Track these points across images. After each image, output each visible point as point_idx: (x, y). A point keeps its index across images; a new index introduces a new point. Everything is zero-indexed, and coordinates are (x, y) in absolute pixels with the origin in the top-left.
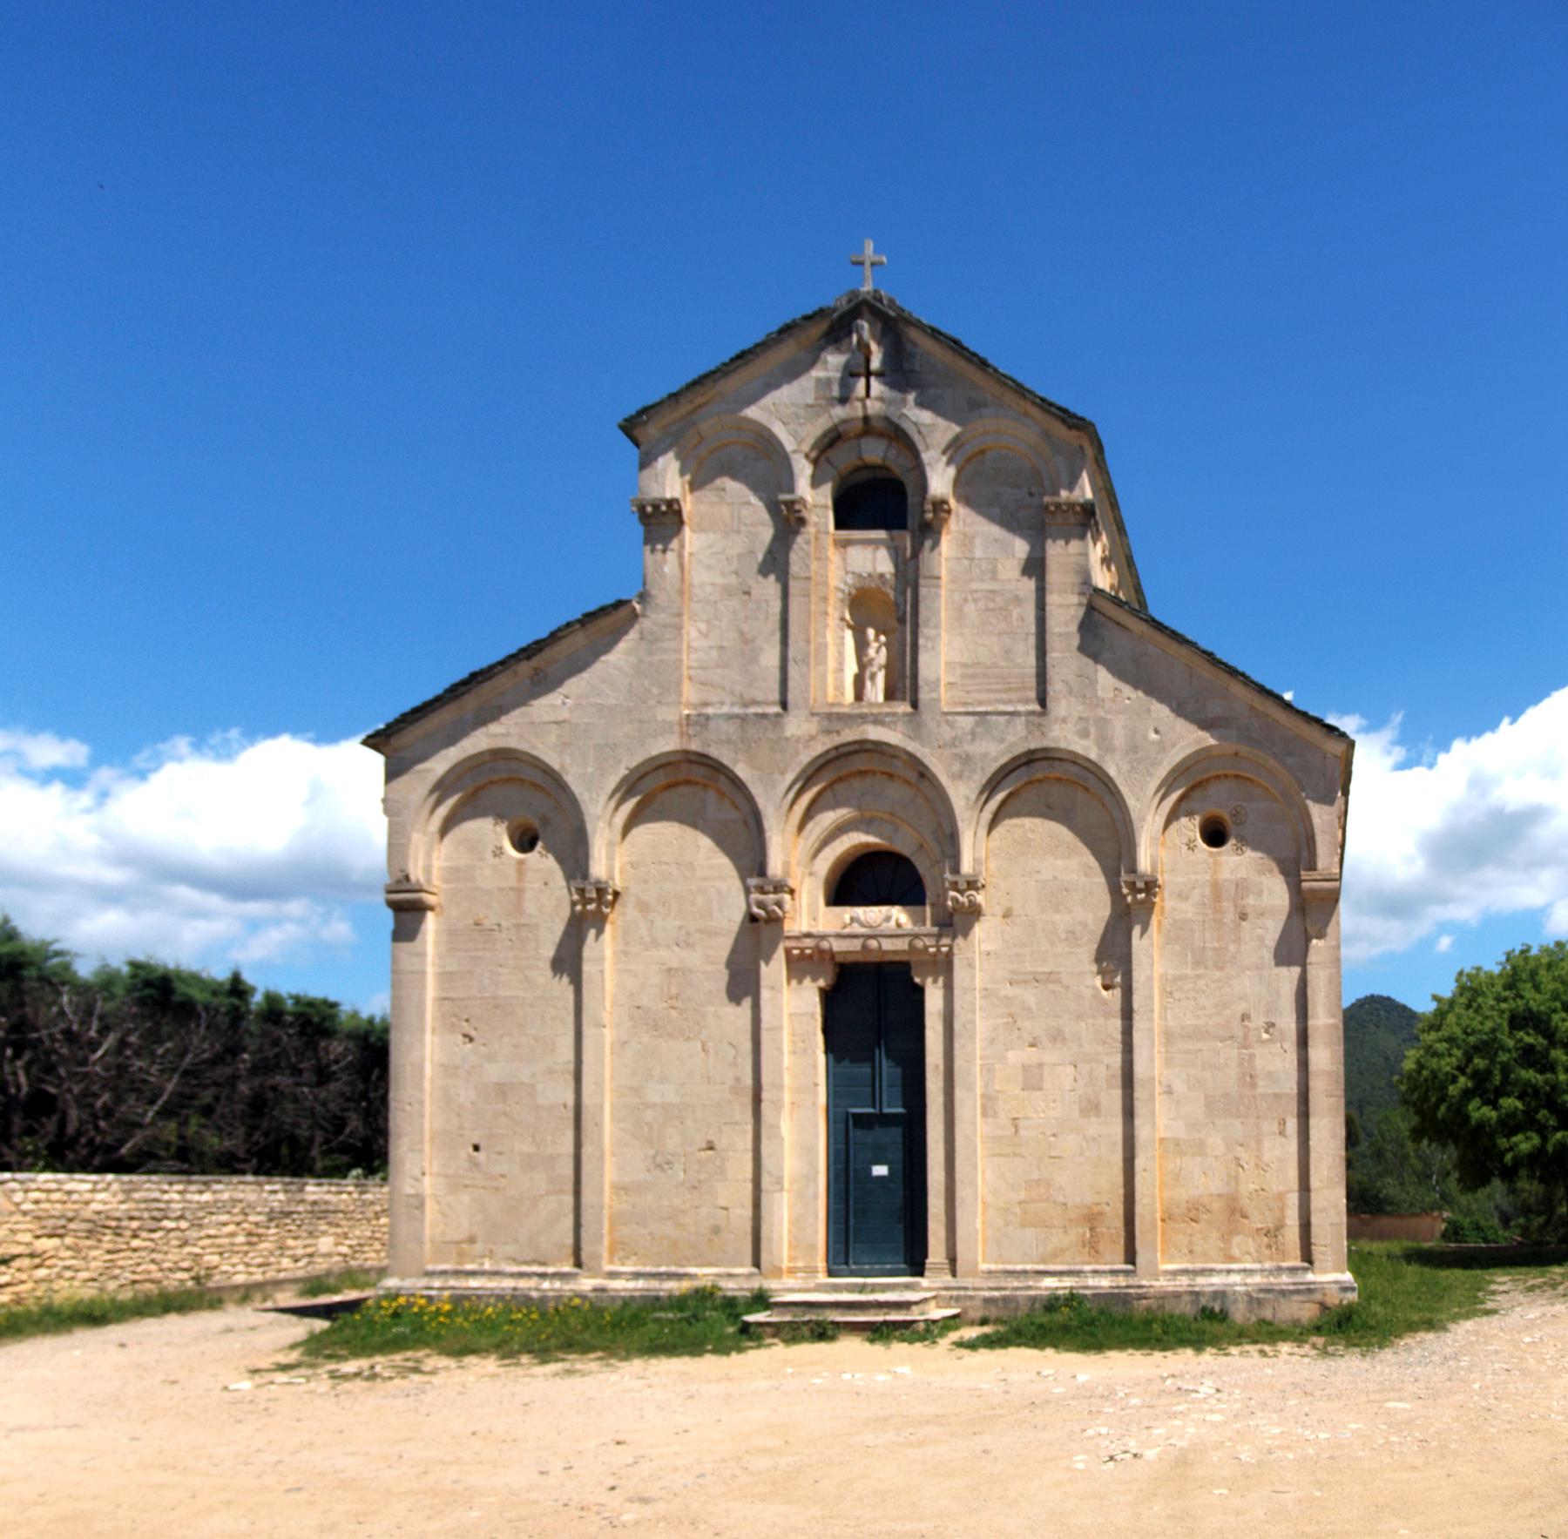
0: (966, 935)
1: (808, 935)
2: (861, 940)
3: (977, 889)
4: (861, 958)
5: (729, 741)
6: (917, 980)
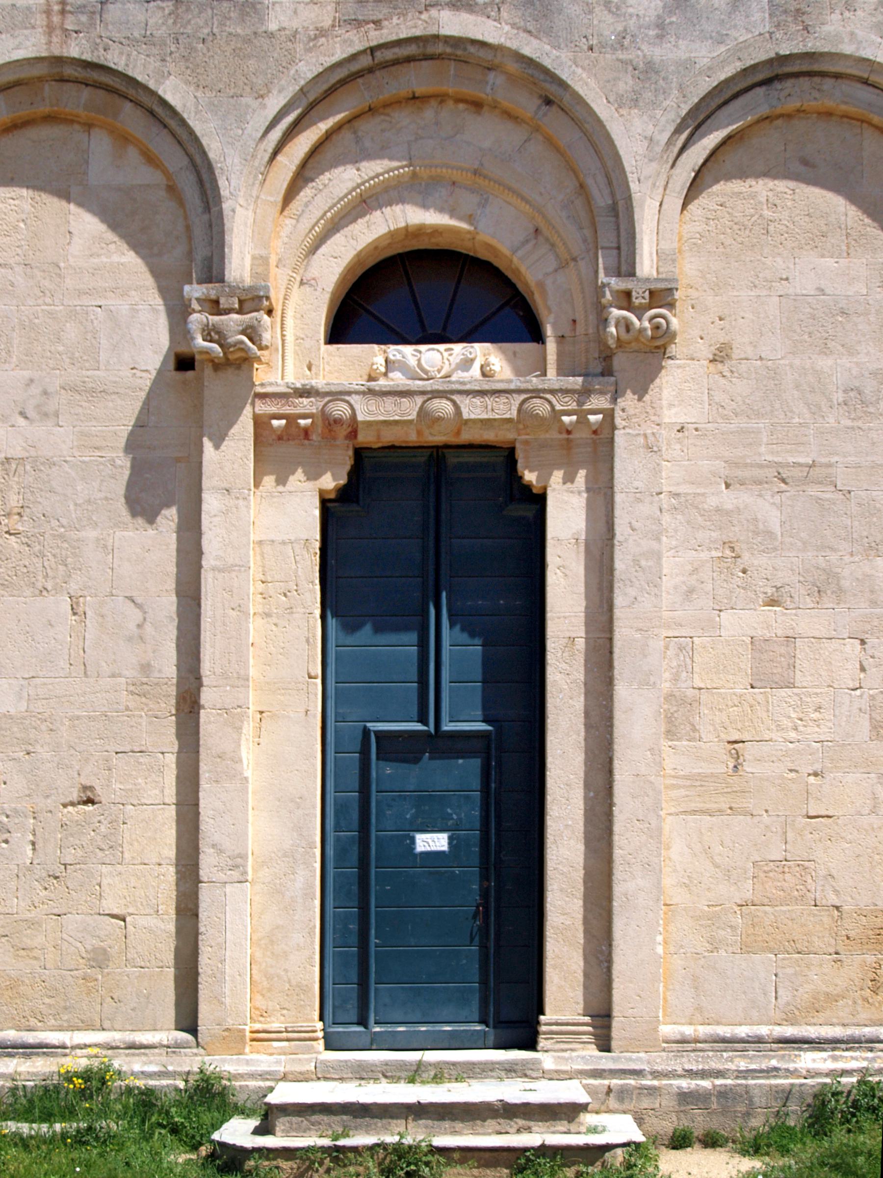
0: (641, 392)
1: (305, 392)
2: (419, 400)
3: (671, 306)
4: (412, 438)
5: (148, 40)
6: (530, 477)
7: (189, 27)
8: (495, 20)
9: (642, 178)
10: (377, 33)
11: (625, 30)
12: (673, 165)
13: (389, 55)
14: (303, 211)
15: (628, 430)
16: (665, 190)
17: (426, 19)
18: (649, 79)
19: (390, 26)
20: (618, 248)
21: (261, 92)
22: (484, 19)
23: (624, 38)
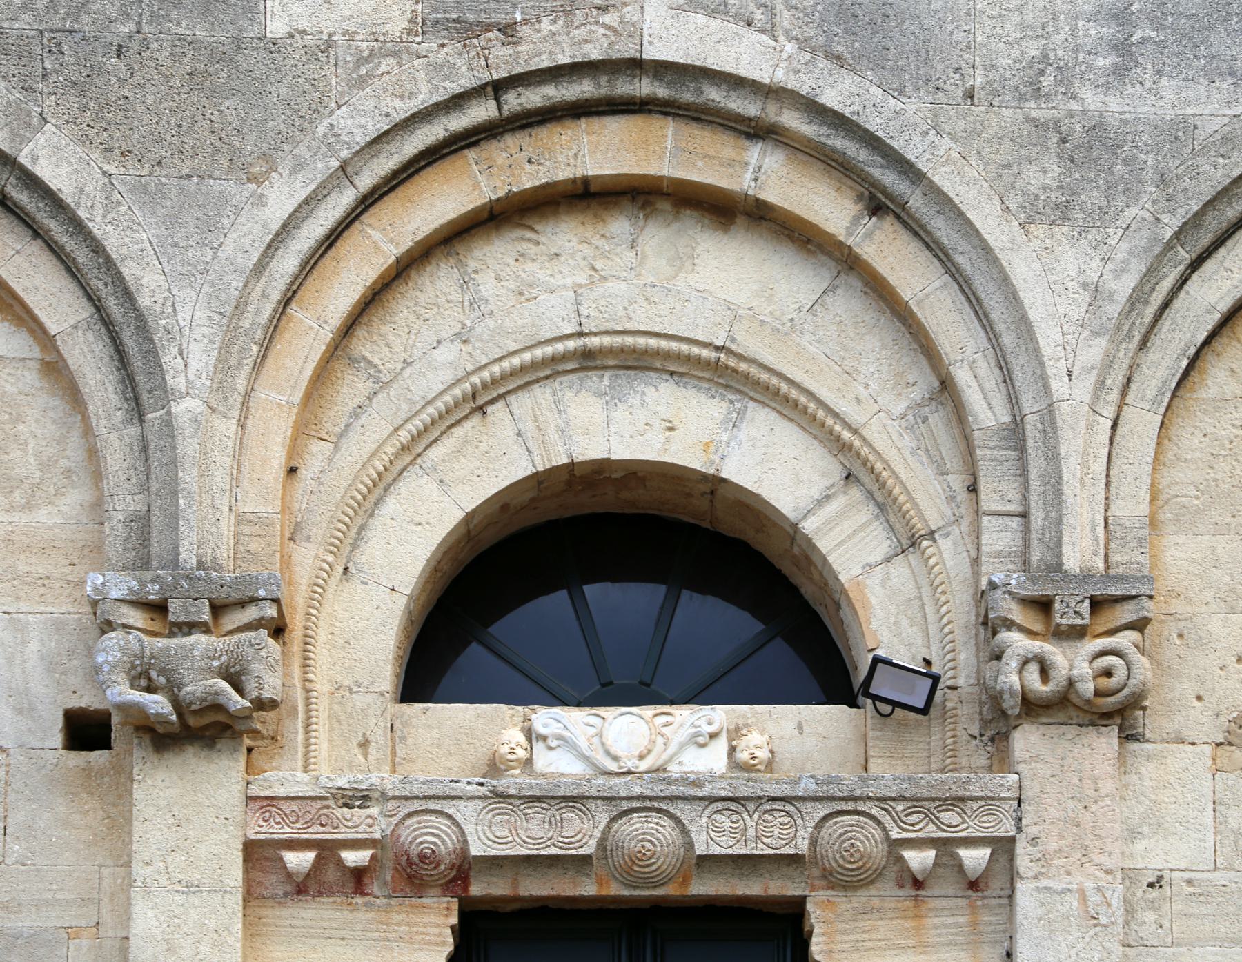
7: (85, 18)
8: (763, 31)
9: (1076, 370)
10: (509, 50)
11: (1045, 56)
12: (1144, 344)
13: (534, 98)
14: (348, 426)
16: (1124, 394)
17: (615, 25)
18: (1096, 161)
19: (536, 37)
20: (1024, 515)
21: (255, 170)
22: (742, 30)
23: (1042, 73)
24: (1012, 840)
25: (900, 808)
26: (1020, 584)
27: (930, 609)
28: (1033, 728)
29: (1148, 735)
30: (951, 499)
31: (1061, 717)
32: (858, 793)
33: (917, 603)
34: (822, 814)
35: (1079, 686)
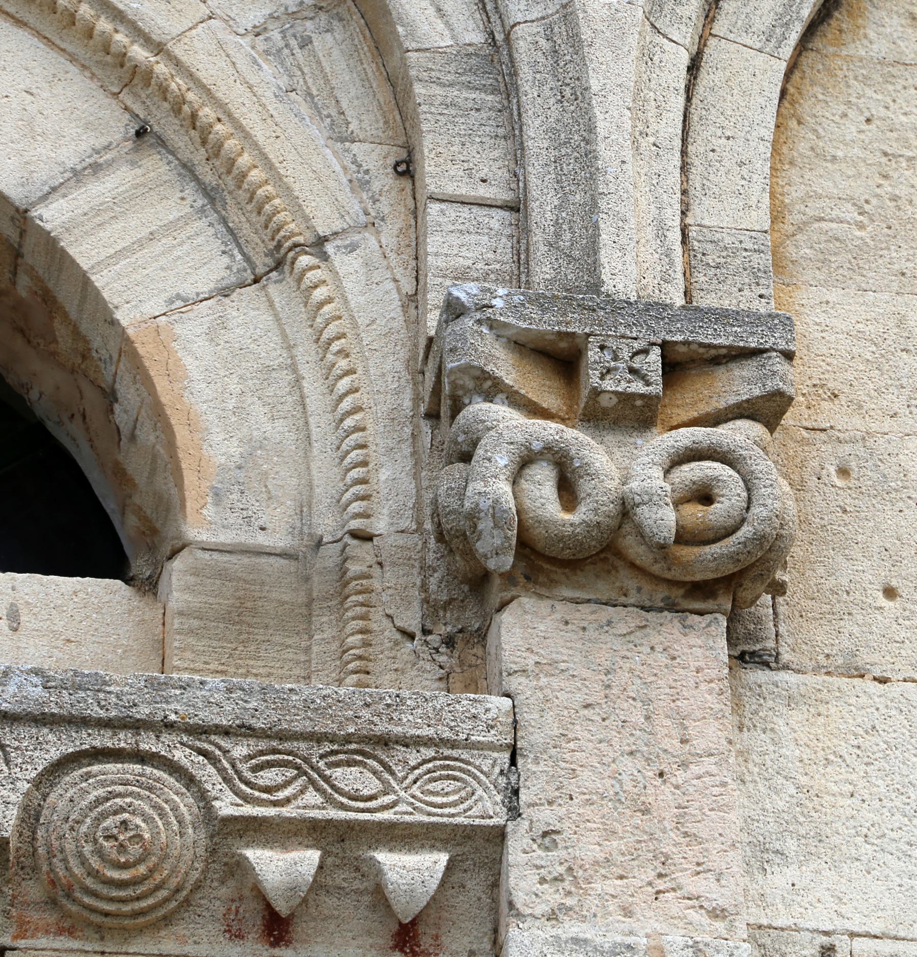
15: (571, 928)
24: (499, 836)
25: (240, 750)
26: (513, 308)
27: (313, 388)
28: (544, 606)
29: (786, 656)
30: (360, 184)
31: (604, 590)
32: (143, 712)
33: (287, 377)
34: (54, 754)
35: (645, 514)
